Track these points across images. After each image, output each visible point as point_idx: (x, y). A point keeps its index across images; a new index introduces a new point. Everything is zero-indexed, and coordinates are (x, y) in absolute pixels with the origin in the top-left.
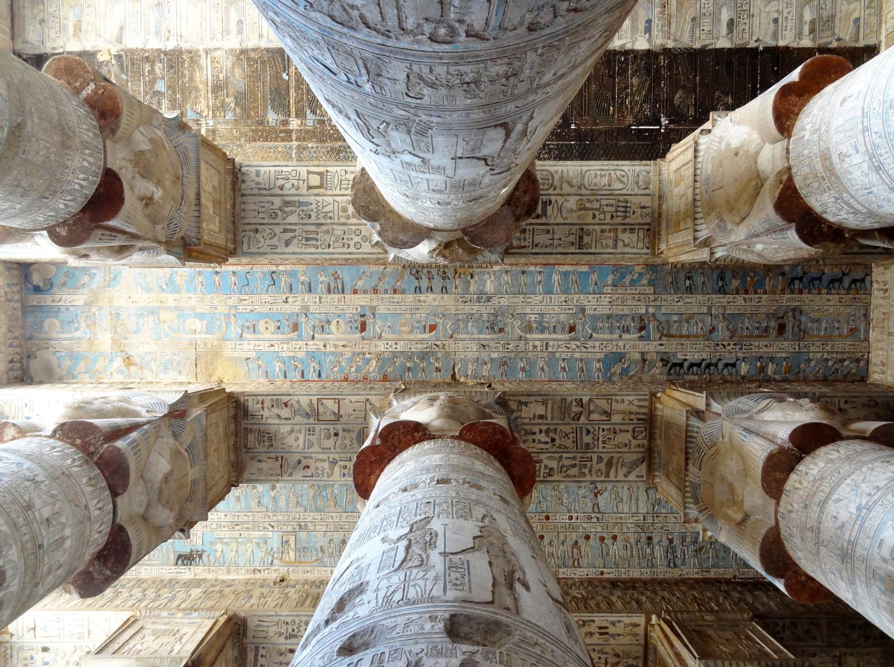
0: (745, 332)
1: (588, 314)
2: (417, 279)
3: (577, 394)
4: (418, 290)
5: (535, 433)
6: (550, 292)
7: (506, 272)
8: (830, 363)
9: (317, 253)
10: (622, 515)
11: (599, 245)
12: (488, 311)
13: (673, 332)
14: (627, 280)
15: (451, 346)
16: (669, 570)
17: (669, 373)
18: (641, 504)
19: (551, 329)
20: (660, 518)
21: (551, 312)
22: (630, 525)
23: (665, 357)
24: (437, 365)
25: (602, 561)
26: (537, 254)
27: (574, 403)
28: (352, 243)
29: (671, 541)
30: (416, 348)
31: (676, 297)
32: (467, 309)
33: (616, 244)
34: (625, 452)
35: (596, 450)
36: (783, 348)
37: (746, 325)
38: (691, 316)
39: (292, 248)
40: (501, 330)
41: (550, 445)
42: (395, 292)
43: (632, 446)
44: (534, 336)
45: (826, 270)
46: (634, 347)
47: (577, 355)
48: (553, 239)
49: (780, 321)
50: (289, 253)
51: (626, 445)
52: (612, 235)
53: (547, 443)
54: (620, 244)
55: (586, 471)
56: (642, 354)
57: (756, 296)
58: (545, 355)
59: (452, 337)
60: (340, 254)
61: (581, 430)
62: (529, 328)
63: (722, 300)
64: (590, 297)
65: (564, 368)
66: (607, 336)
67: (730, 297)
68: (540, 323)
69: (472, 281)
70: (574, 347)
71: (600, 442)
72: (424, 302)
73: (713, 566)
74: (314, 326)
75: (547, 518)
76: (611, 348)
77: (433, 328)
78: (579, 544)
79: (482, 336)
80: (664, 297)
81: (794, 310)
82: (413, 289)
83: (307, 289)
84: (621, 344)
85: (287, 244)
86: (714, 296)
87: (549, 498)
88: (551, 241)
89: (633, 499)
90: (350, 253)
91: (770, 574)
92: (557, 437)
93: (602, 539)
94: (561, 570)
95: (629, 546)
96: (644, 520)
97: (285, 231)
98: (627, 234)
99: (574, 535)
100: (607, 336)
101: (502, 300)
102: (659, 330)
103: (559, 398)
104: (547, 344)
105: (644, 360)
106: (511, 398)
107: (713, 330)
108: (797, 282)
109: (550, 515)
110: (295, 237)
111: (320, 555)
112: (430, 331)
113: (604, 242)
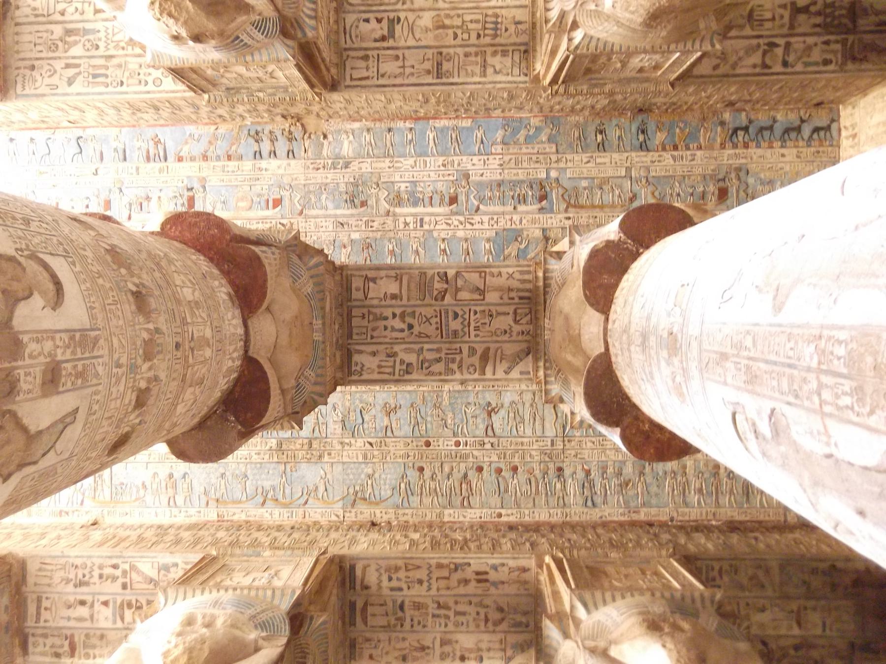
1: (473, 181)
2: (257, 141)
3: (439, 266)
4: (258, 155)
5: (386, 318)
7: (368, 130)
9: (107, 93)
10: (525, 440)
11: (462, 73)
12: (346, 180)
13: (582, 201)
14: (521, 136)
16: (586, 510)
18: (547, 425)
19: (427, 200)
21: (425, 179)
22: (534, 453)
25: (499, 500)
26: (384, 86)
27: (437, 278)
28: (150, 79)
29: (588, 473)
31: (585, 157)
32: (320, 177)
33: (485, 71)
34: (505, 342)
35: (466, 338)
37: (677, 190)
38: (606, 181)
39: (77, 87)
40: (364, 204)
41: (406, 332)
42: (229, 158)
43: (514, 334)
45: (779, 117)
46: (533, 221)
47: (460, 234)
48: (403, 67)
49: (721, 184)
50: (72, 94)
51: (506, 332)
52: (479, 59)
53: (402, 331)
54: (490, 71)
55: (455, 366)
56: (544, 230)
57: (688, 153)
58: (419, 234)
59: (301, 213)
60: (136, 93)
61: (447, 312)
62: (398, 200)
63: (644, 159)
64: (475, 159)
65: (444, 251)
67: (653, 155)
68: (412, 194)
69: (326, 142)
70: (456, 223)
71: (472, 328)
73: (644, 505)
74: (130, 205)
75: (428, 444)
77: (277, 203)
79: (339, 212)
80: (569, 157)
81: (738, 169)
82: (251, 155)
83: (122, 157)
84: (516, 218)
85: (70, 82)
86: (634, 154)
87: (429, 419)
88: (402, 70)
89: (537, 418)
90: (148, 92)
91: (599, 420)
92: (415, 322)
93: (499, 471)
94: (447, 512)
95: (533, 480)
96: (552, 444)
97: (68, 66)
98: (498, 57)
99: (463, 466)
100: (498, 208)
101: (363, 166)
102: (564, 199)
103: (417, 272)
104: (422, 220)
105: (547, 239)
106: (357, 273)
108: (741, 133)
109: (431, 440)
110: (80, 73)
111: (142, 492)
112: (275, 207)
113: (469, 68)
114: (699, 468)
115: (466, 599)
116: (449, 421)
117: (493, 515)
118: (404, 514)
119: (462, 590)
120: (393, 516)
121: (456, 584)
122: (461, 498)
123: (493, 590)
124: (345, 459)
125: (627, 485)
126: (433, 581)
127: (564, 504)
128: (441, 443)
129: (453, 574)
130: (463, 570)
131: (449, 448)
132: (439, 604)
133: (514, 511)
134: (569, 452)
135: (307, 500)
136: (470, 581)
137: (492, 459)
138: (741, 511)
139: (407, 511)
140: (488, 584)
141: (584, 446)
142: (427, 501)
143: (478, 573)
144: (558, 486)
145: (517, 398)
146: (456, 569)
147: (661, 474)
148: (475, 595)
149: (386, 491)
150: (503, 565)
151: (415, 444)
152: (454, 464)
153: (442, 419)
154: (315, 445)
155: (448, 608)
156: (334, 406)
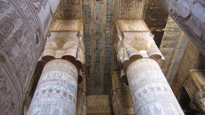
0: (96, 79)
4: (107, 15)
6: (106, 44)
7: (111, 36)
8: (90, 91)
14: (107, 59)
15: (92, 23)
17: (87, 67)
23: (90, 66)
24: (87, 20)
30: (92, 15)
36: (93, 83)
38: (99, 70)
44: (95, 42)
47: (90, 50)
54: (116, 65)
59: (95, 23)
62: (97, 40)
66: (95, 56)
72: (104, 17)
76: (92, 57)
77: (97, 19)
79: (95, 30)
82: (108, 14)
86: (103, 73)
100: (95, 56)
105: (90, 63)
107: (96, 74)
112: (96, 18)
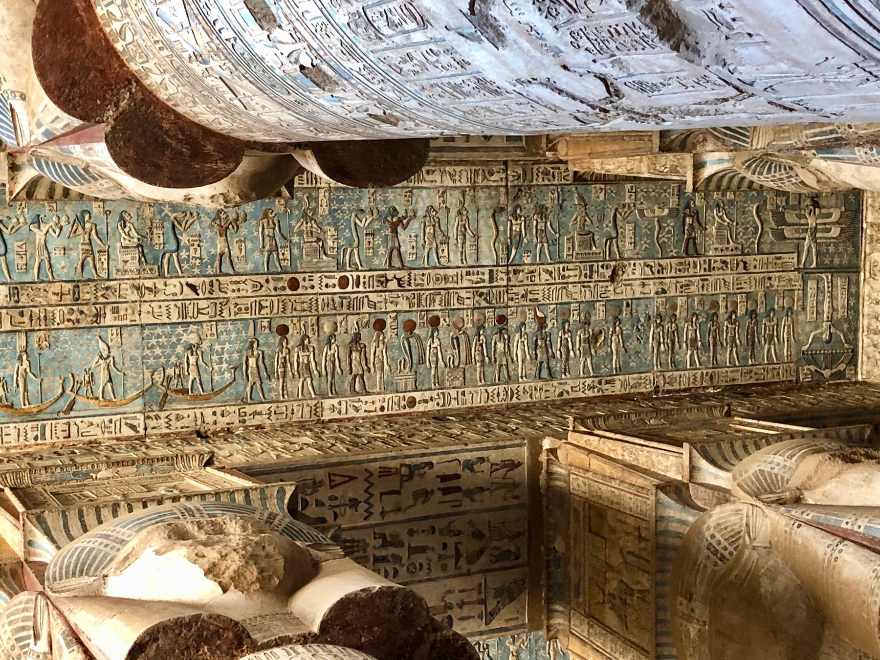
16: (540, 384)
20: (521, 276)
22: (463, 294)
29: (542, 323)
73: (620, 371)
75: (294, 284)
78: (364, 341)
87: (295, 239)
93: (410, 327)
94: (327, 403)
95: (462, 339)
96: (491, 280)
99: (353, 319)
109: (299, 277)
114: (693, 308)
115: (426, 525)
116: (330, 243)
117: (403, 403)
118: (256, 413)
119: (420, 510)
120: (236, 419)
121: (411, 502)
122: (350, 377)
123: (467, 505)
124: (146, 319)
125: (596, 341)
126: (375, 500)
127: (509, 377)
128: (316, 283)
129: (405, 484)
130: (422, 476)
131: (330, 290)
132: (383, 536)
133: (434, 394)
134: (515, 290)
135: (74, 402)
136: (432, 491)
137: (399, 308)
138: (745, 369)
139: (259, 408)
140: (459, 495)
141: (537, 281)
142: (295, 386)
143: (444, 478)
144: (500, 346)
145: (437, 202)
146: (411, 476)
147: (642, 320)
148: (438, 516)
149: (221, 373)
150: (482, 460)
151: (271, 285)
152: (339, 318)
153: (319, 240)
154: (87, 292)
155: (399, 544)
156: (122, 218)
